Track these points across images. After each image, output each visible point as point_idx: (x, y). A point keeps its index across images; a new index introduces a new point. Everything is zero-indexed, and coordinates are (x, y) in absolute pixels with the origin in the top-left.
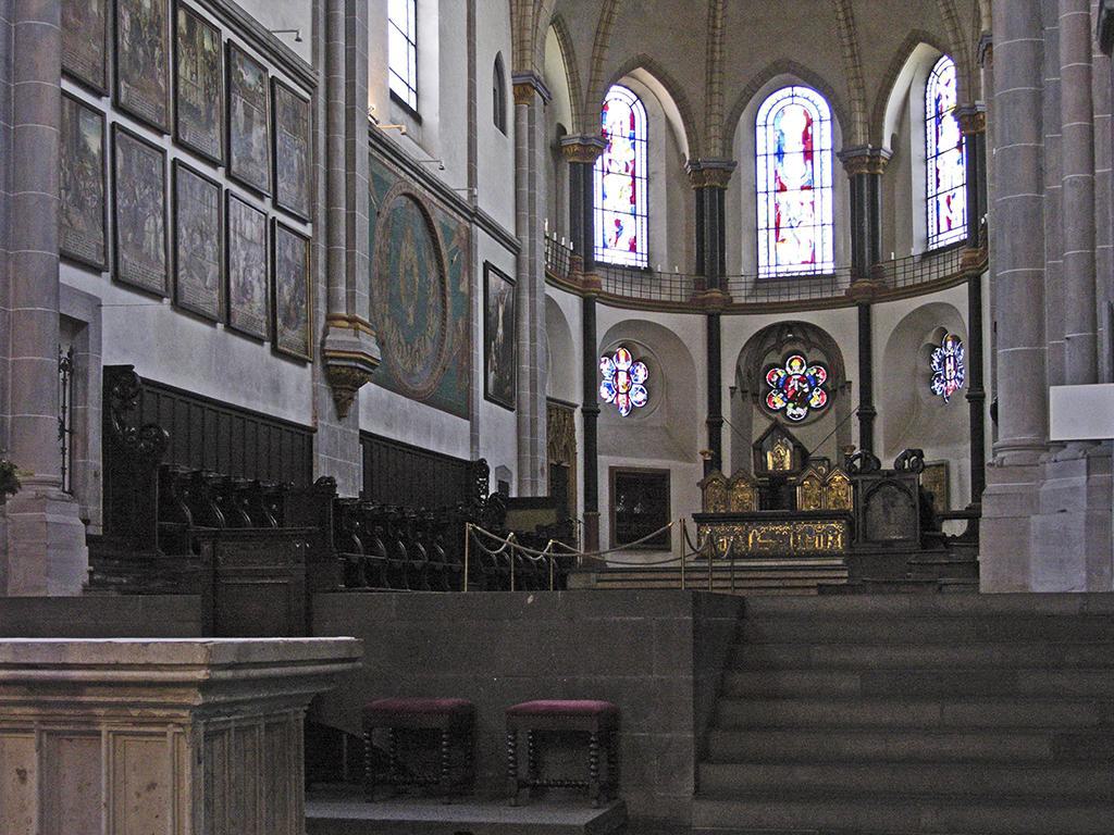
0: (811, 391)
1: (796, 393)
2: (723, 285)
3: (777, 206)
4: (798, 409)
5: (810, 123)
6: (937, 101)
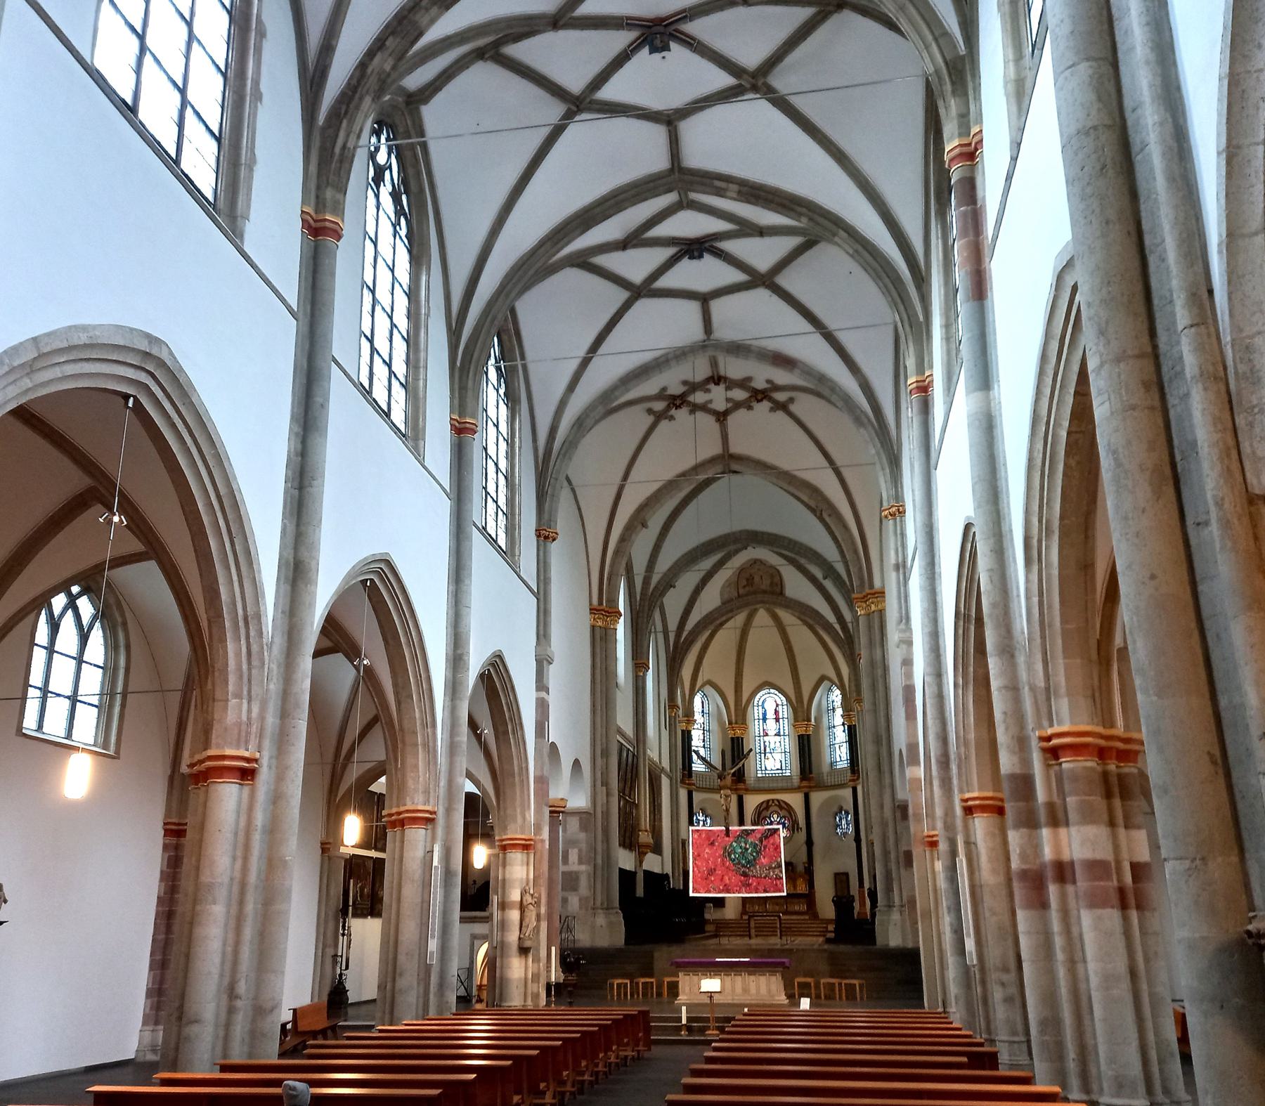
5: (777, 705)
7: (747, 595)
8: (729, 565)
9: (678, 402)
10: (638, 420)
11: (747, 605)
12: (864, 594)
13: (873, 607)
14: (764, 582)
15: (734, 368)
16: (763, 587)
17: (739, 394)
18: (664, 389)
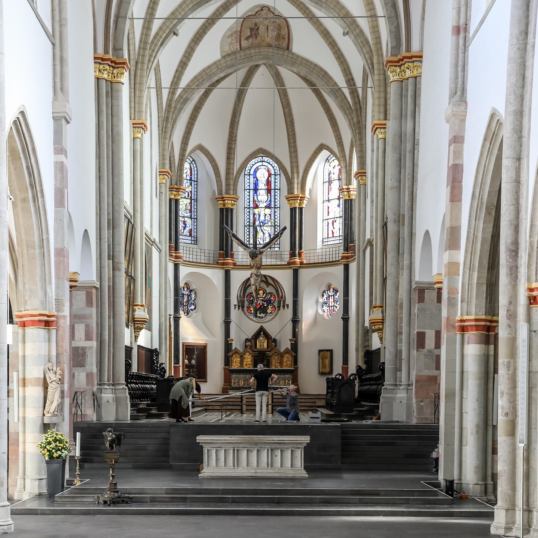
1: (261, 306)
2: (232, 256)
4: (262, 314)
5: (270, 175)
6: (329, 174)
11: (250, 58)
12: (399, 57)
13: (408, 73)
14: (270, 35)
16: (268, 40)
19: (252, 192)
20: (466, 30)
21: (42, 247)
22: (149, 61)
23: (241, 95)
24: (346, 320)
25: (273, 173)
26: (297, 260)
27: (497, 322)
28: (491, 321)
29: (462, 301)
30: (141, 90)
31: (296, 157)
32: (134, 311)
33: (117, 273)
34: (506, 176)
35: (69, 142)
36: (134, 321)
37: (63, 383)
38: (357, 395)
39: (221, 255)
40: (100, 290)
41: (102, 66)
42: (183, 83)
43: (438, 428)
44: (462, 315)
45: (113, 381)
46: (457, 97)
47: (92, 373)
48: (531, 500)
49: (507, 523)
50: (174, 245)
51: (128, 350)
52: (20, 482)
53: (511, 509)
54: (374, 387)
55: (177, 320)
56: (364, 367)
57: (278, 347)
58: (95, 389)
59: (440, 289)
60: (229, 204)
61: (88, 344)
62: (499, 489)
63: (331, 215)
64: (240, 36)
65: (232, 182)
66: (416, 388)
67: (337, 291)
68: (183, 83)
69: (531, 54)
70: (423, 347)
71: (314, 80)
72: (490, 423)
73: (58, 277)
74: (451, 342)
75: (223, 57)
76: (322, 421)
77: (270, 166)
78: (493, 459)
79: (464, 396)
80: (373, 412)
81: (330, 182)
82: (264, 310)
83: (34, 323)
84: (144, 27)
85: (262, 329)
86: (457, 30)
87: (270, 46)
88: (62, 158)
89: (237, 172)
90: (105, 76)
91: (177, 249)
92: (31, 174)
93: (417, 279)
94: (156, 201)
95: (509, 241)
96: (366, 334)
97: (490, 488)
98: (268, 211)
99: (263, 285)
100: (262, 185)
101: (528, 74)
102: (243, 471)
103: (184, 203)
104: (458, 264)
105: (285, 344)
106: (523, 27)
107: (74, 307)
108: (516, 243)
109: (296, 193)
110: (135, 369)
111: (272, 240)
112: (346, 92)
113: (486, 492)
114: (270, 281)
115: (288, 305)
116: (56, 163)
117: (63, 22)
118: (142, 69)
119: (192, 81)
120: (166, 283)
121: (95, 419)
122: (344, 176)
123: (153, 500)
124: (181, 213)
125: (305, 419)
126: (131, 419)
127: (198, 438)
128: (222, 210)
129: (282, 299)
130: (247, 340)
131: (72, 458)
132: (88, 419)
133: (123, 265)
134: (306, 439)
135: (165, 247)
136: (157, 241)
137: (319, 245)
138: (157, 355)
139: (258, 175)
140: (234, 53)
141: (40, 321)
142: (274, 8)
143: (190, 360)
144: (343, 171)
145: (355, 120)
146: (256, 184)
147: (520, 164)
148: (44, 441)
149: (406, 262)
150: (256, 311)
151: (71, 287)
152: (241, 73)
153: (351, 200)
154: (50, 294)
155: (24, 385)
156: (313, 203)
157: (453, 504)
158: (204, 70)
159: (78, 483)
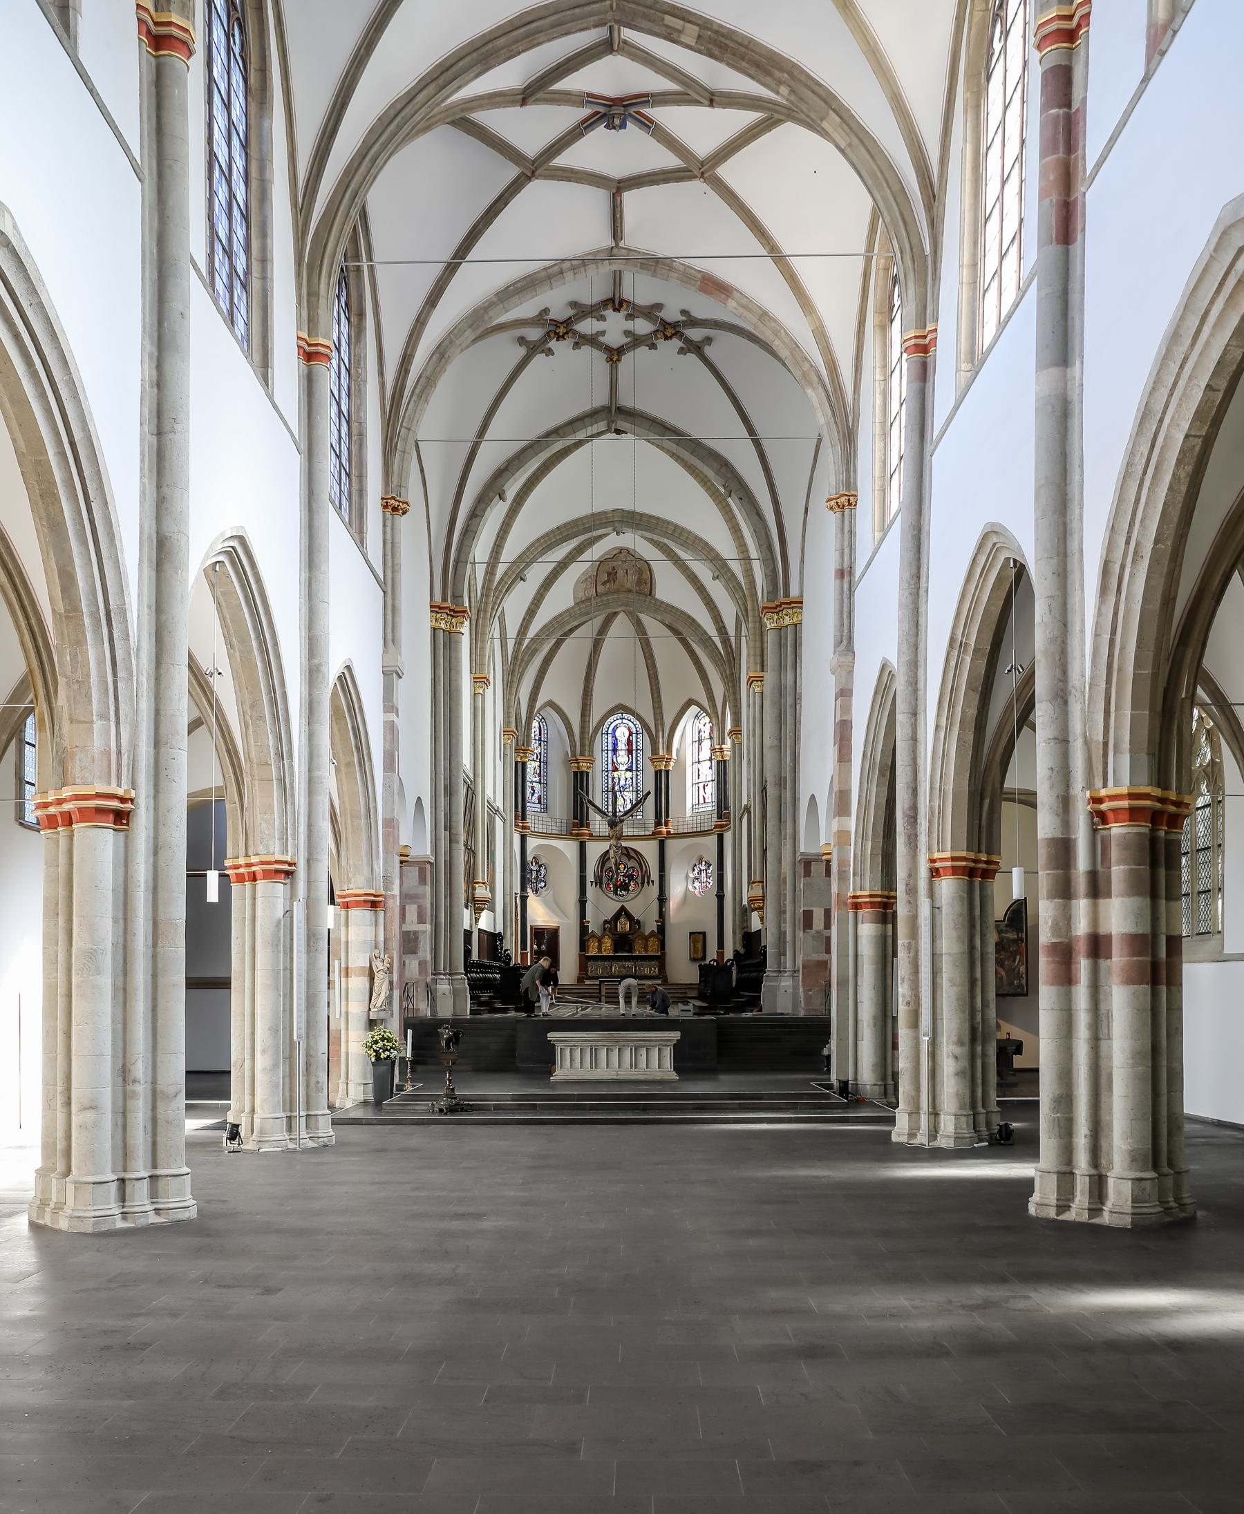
0: (630, 882)
2: (588, 825)
3: (613, 778)
5: (631, 734)
7: (606, 594)
8: (587, 555)
9: (562, 330)
10: (506, 352)
13: (787, 620)
15: (640, 289)
16: (628, 585)
17: (643, 327)
18: (546, 311)
19: (610, 752)
20: (851, 573)
21: (368, 816)
22: (493, 609)
23: (597, 645)
24: (720, 897)
25: (634, 731)
26: (664, 829)
27: (895, 898)
28: (888, 897)
29: (854, 875)
30: (483, 641)
31: (661, 713)
32: (474, 889)
33: (454, 846)
34: (901, 733)
35: (401, 699)
36: (474, 900)
37: (391, 973)
38: (734, 983)
39: (575, 825)
40: (435, 866)
41: (439, 615)
42: (532, 633)
43: (829, 1020)
44: (854, 890)
45: (450, 970)
46: (842, 647)
47: (425, 962)
48: (938, 1102)
49: (910, 1129)
50: (521, 813)
51: (468, 934)
52: (342, 1087)
53: (914, 1113)
54: (754, 974)
55: (524, 899)
56: (742, 951)
57: (642, 930)
58: (429, 980)
59: (829, 861)
60: (584, 766)
61: (421, 927)
62: (901, 1089)
63: (702, 779)
64: (596, 581)
65: (587, 743)
66: (803, 974)
67: (710, 865)
68: (532, 633)
69: (924, 600)
70: (811, 928)
71: (680, 628)
72: (889, 1014)
73: (386, 851)
74: (843, 922)
75: (577, 604)
76: (694, 1014)
77: (631, 724)
78: (893, 1055)
79: (859, 984)
80: (754, 1003)
81: (700, 741)
82: (625, 887)
83: (358, 904)
84: (486, 572)
85: (623, 909)
86: (841, 574)
87: (630, 591)
88: (393, 717)
89: (594, 731)
90: (443, 626)
91: (524, 818)
92: (357, 735)
93: (802, 850)
94: (500, 764)
95: (906, 806)
96: (744, 914)
97: (891, 1090)
98: (629, 774)
99: (625, 859)
100: (622, 745)
101: (922, 621)
102: (602, 1073)
103: (532, 766)
104: (849, 832)
105: (651, 926)
106: (914, 570)
107: (405, 885)
108: (914, 808)
109: (661, 754)
110: (475, 956)
111: (633, 807)
112: (717, 641)
113: (886, 1094)
114: (632, 854)
115: (653, 881)
116: (385, 722)
117: (396, 568)
118: (484, 618)
119: (541, 630)
120: (511, 858)
121: (429, 1014)
122: (716, 735)
123: (498, 1108)
124: (529, 777)
125: (675, 1012)
126: (471, 1014)
127: (549, 1035)
128: (576, 773)
129: (646, 877)
130: (606, 922)
131: (402, 1059)
132: (421, 1014)
133: (462, 838)
134: (676, 1035)
135: (510, 816)
136: (501, 809)
137: (689, 812)
138: (501, 940)
139: (618, 733)
140: (589, 599)
141: (365, 901)
142: (635, 551)
143: (539, 946)
144: (715, 728)
145: (728, 672)
146: (615, 744)
147: (916, 720)
148: (370, 1040)
149: (789, 831)
150: (616, 888)
151: (401, 862)
152: (598, 622)
153: (725, 761)
154: (378, 870)
155: (347, 975)
156: (681, 765)
157: (848, 1108)
158: (555, 618)
159: (409, 1088)
